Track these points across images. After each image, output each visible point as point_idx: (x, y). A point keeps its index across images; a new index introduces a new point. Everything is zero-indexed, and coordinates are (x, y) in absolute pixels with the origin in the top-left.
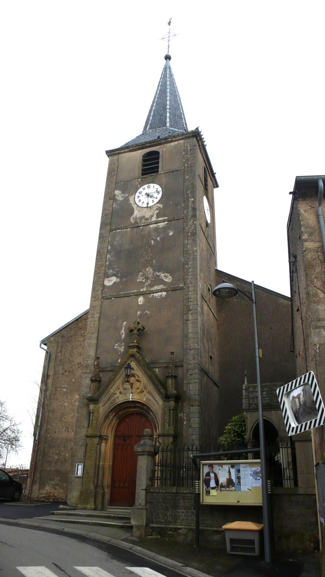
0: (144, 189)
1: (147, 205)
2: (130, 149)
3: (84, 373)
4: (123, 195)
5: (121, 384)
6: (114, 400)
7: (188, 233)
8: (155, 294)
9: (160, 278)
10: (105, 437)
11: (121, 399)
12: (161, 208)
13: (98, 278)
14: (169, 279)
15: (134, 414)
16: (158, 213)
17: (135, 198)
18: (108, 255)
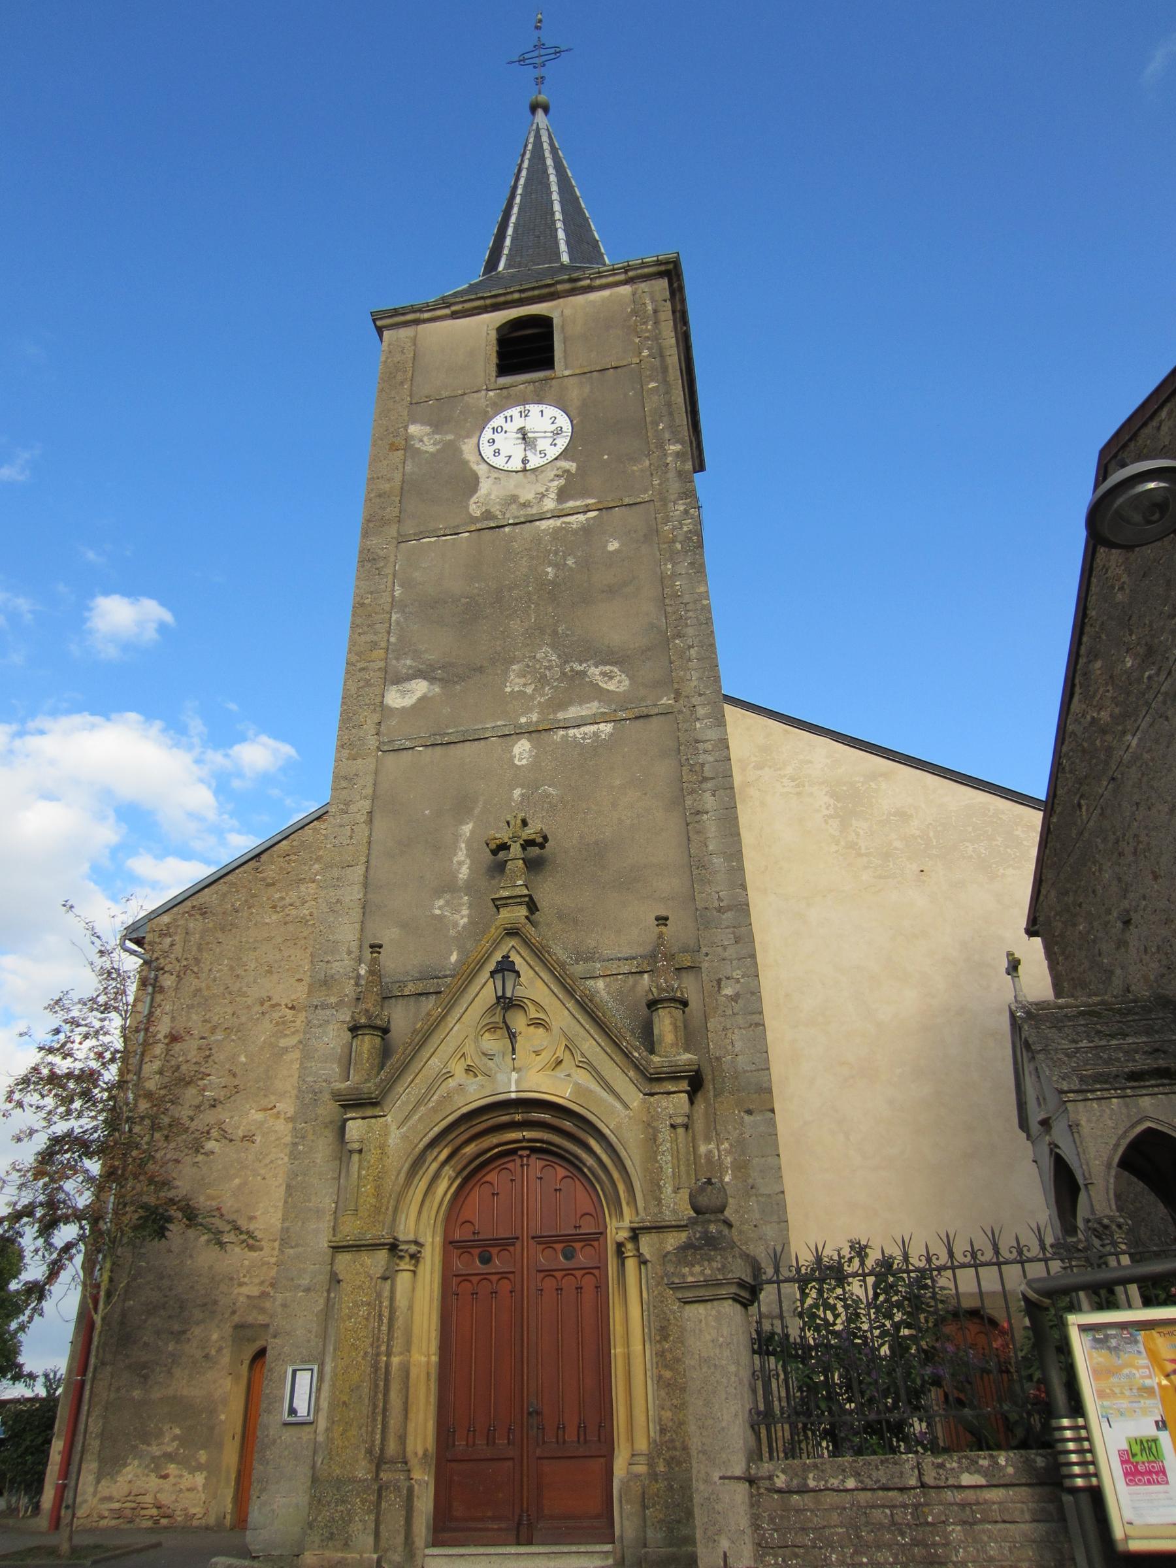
0: (509, 419)
1: (522, 465)
2: (454, 308)
3: (316, 1007)
4: (437, 437)
5: (472, 1037)
6: (448, 1097)
7: (674, 541)
8: (571, 732)
9: (588, 680)
10: (413, 1248)
11: (475, 1094)
12: (573, 472)
13: (362, 684)
14: (620, 682)
15: (520, 1153)
16: (565, 485)
17: (481, 446)
18: (395, 613)
